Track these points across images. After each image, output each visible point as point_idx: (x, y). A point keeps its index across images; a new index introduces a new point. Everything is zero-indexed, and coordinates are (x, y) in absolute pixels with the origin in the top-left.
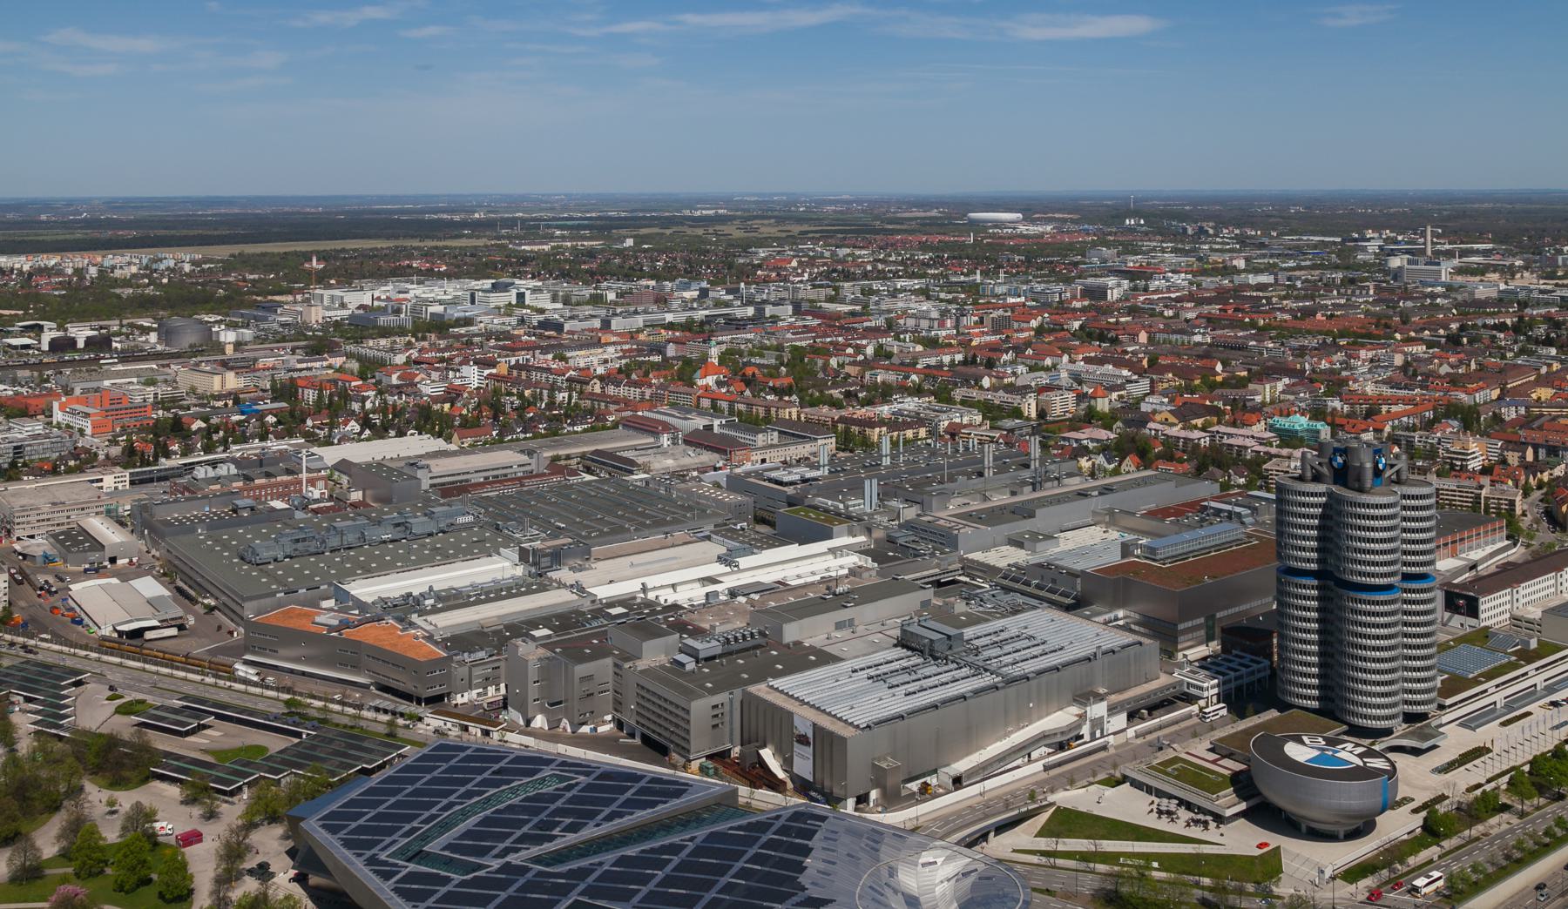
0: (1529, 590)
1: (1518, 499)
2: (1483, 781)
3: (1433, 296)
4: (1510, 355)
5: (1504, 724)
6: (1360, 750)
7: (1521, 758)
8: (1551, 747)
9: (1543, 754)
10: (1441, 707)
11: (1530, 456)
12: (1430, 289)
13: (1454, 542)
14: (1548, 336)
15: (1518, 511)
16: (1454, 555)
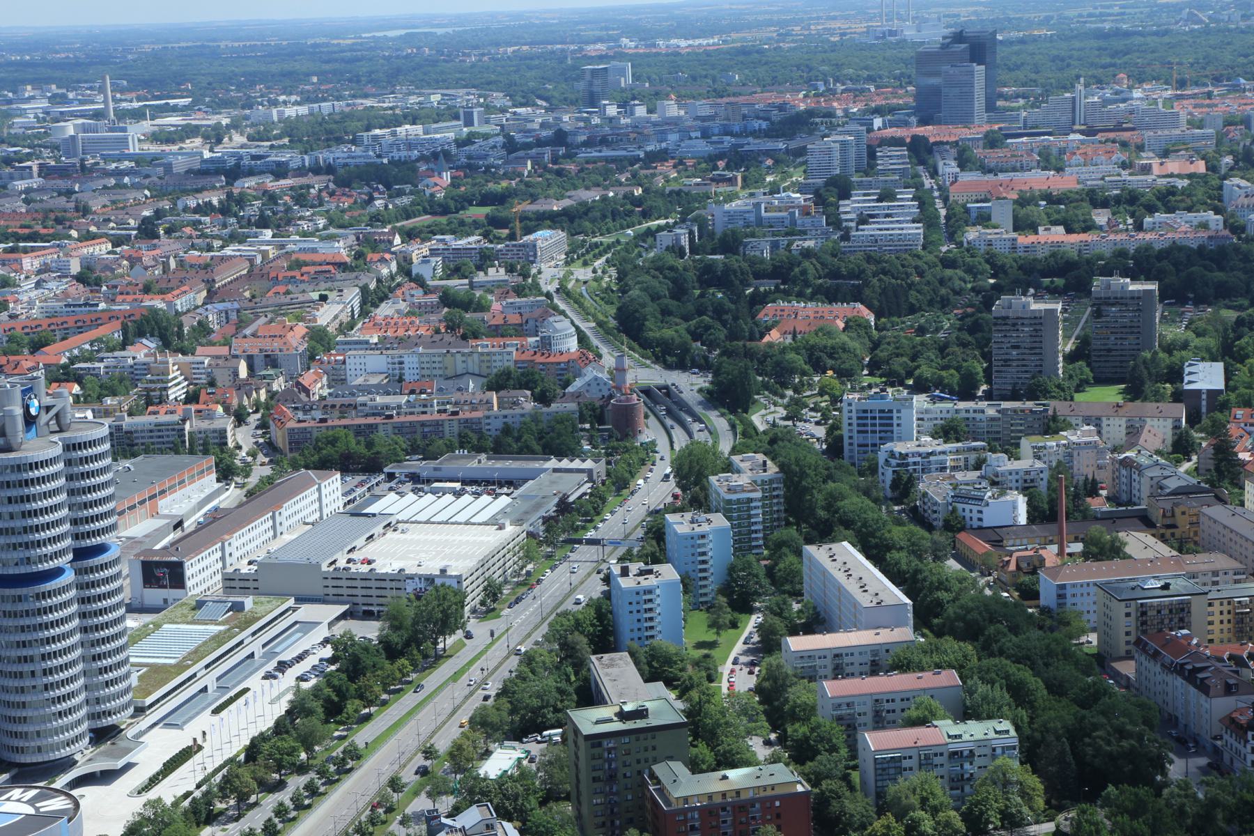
0: (243, 540)
1: (229, 428)
2: (192, 787)
3: (119, 173)
4: (217, 243)
5: (216, 711)
6: (33, 793)
7: (237, 746)
8: (271, 724)
9: (262, 734)
10: (140, 711)
11: (243, 372)
12: (114, 165)
13: (151, 498)
14: (262, 216)
15: (231, 444)
16: (155, 514)
